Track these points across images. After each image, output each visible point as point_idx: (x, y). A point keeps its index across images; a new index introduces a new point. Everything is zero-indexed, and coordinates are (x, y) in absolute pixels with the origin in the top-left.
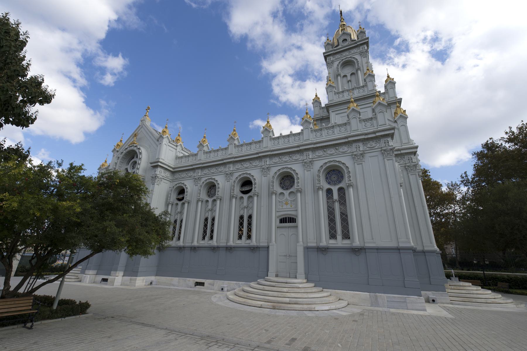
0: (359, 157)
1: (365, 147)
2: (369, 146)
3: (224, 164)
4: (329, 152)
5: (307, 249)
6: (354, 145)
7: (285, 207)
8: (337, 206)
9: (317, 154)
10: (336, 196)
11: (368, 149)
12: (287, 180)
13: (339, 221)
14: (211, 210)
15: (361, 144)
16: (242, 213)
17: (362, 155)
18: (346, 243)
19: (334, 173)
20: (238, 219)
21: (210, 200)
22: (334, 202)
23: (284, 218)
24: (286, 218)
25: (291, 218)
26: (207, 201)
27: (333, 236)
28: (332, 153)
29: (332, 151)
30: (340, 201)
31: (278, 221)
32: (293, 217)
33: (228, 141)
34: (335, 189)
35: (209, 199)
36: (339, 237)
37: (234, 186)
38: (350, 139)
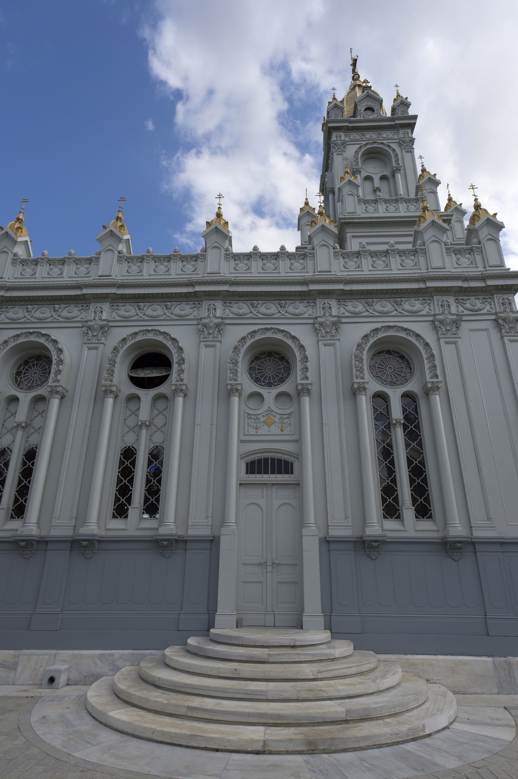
0: (447, 327)
1: (461, 309)
2: (468, 306)
3: (83, 300)
4: (378, 307)
5: (327, 542)
6: (437, 299)
7: (264, 430)
8: (399, 436)
9: (350, 308)
10: (397, 413)
14: (25, 427)
16: (130, 440)
18: (425, 529)
20: (116, 457)
21: (25, 398)
26: (14, 400)
27: (391, 510)
30: (405, 427)
33: (100, 240)
34: (395, 396)
35: (20, 395)
36: (408, 511)
37: (113, 363)
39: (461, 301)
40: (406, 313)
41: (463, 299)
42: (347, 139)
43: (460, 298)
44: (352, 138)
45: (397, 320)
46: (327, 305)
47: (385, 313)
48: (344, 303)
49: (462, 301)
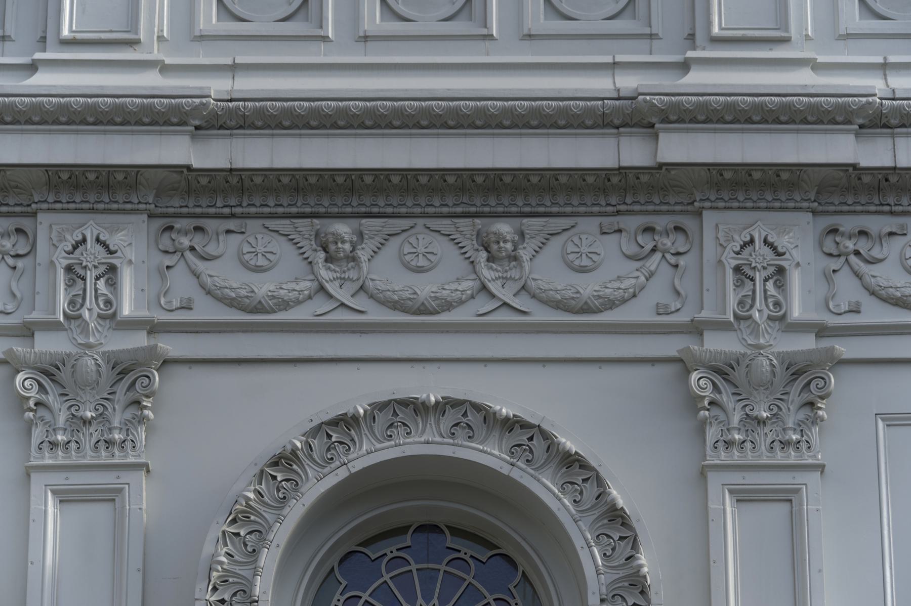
1: (847, 289)
4: (385, 271)
9: (227, 274)
15: (797, 236)
28: (425, 287)
29: (422, 262)
38: (679, 148)
39: (850, 245)
40: (542, 315)
41: (863, 233)
43: (849, 224)
45: (488, 354)
46: (93, 253)
47: (422, 310)
48: (198, 241)
49: (863, 245)
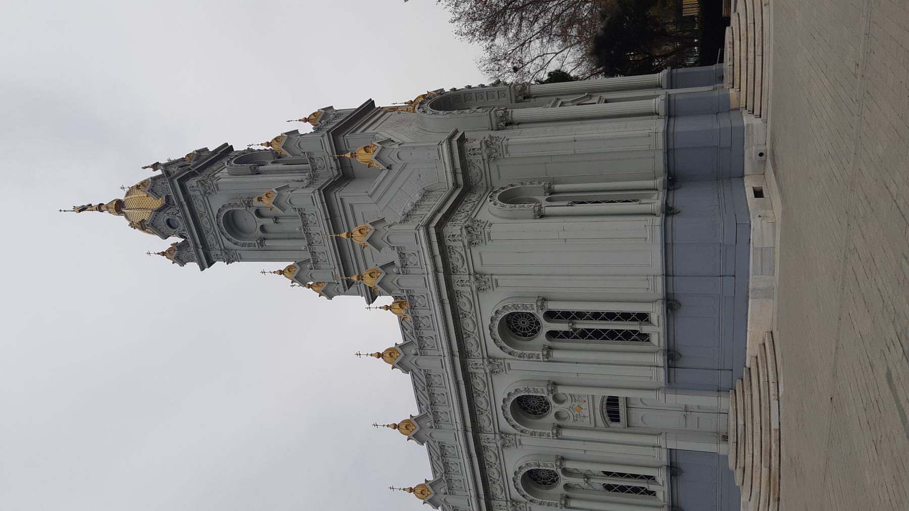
8: (582, 325)
11: (466, 266)
12: (527, 407)
13: (616, 328)
17: (478, 276)
18: (656, 312)
19: (516, 327)
22: (575, 330)
23: (609, 416)
24: (608, 412)
25: (607, 404)
31: (615, 425)
32: (605, 403)
42: (217, 247)
44: (214, 242)
